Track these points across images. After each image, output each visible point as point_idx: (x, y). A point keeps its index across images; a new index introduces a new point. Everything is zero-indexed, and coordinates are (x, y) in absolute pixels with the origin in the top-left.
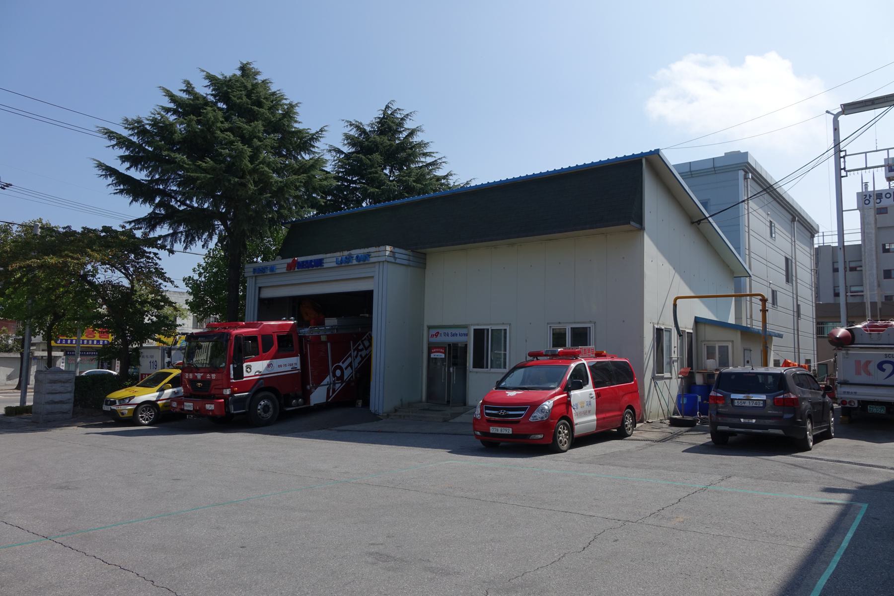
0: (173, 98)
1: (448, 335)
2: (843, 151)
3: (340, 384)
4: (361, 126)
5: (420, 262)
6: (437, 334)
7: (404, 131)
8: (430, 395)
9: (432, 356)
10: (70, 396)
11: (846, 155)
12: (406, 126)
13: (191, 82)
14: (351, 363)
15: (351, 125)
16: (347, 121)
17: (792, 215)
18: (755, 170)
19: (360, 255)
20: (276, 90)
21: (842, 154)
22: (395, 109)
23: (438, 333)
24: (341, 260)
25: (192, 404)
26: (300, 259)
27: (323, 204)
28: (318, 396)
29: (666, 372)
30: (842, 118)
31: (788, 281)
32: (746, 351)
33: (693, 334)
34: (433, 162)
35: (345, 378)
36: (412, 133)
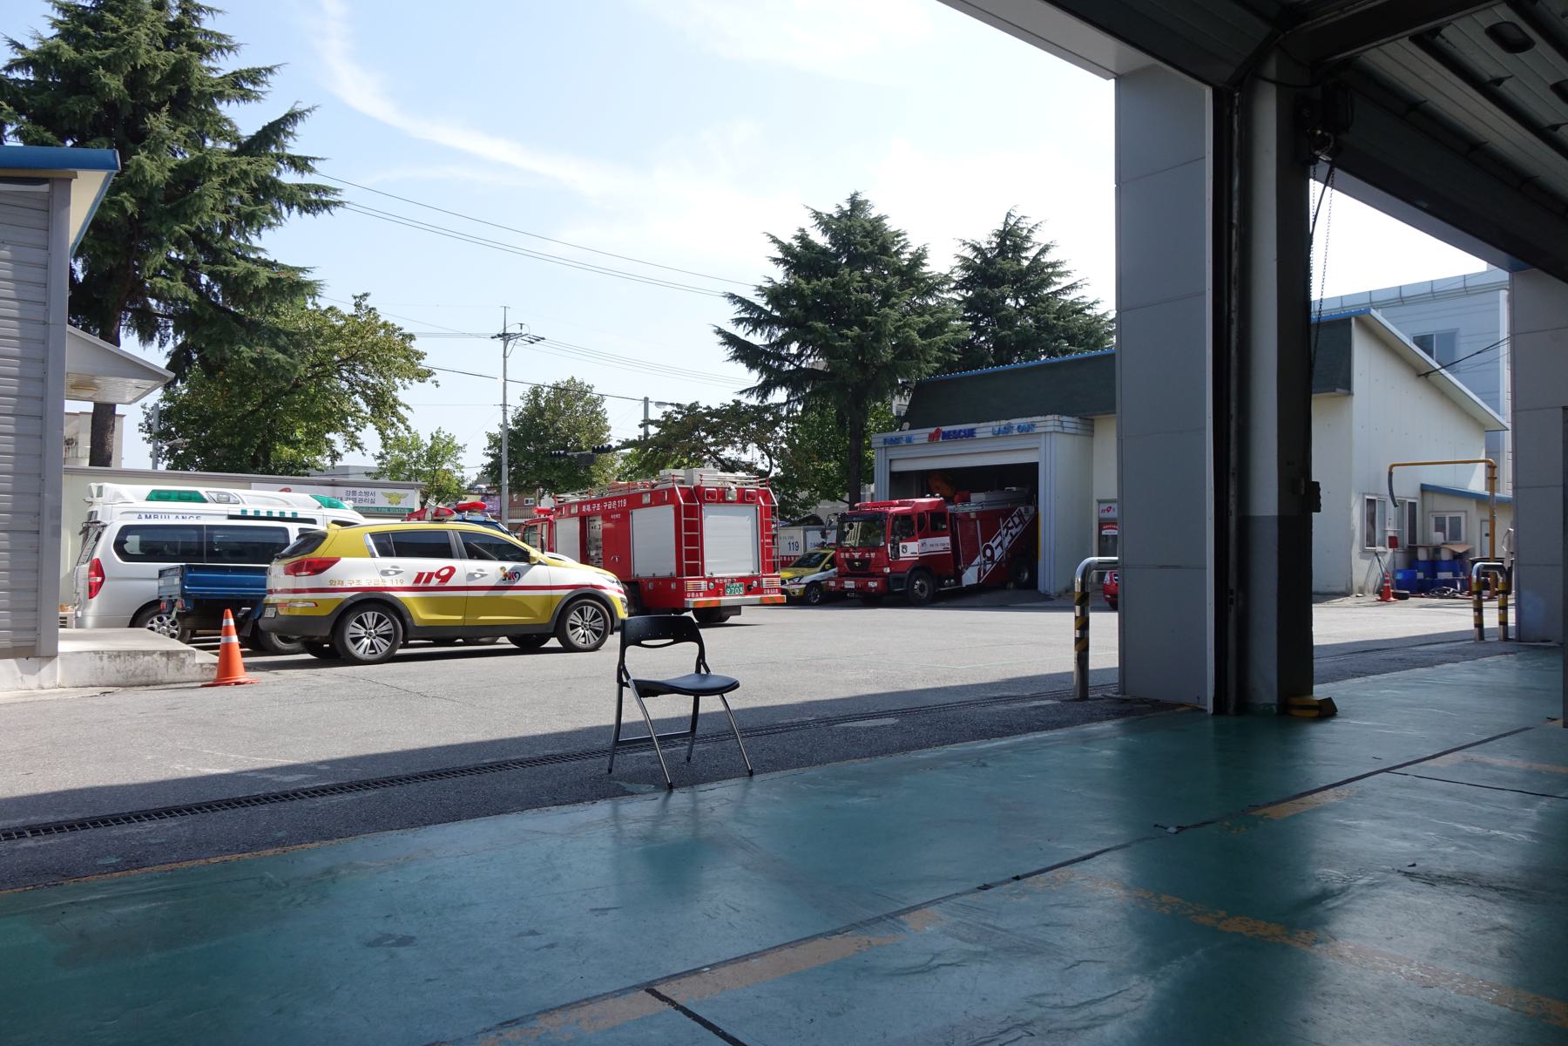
0: (785, 249)
6: (1109, 509)
7: (1032, 247)
9: (1104, 533)
14: (1001, 542)
15: (964, 244)
23: (1110, 508)
26: (945, 429)
27: (957, 360)
32: (1484, 523)
33: (1417, 505)
36: (1044, 251)
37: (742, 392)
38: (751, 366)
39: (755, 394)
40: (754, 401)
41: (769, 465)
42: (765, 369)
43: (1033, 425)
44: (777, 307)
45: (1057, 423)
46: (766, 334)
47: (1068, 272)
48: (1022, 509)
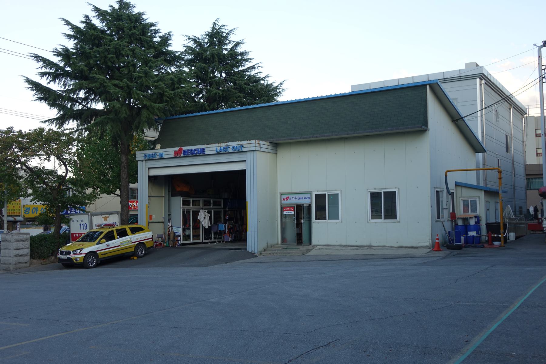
0: (75, 28)
4: (198, 40)
8: (283, 240)
9: (285, 213)
10: (27, 251)
12: (230, 39)
13: (90, 17)
15: (189, 39)
16: (187, 36)
17: (509, 104)
18: (487, 77)
19: (235, 146)
23: (288, 197)
26: (185, 148)
29: (441, 218)
31: (507, 151)
32: (487, 203)
33: (454, 193)
36: (238, 44)
37: (45, 122)
38: (52, 105)
39: (55, 123)
40: (54, 127)
41: (65, 171)
42: (61, 107)
44: (68, 64)
45: (257, 145)
46: (62, 83)
47: (249, 59)
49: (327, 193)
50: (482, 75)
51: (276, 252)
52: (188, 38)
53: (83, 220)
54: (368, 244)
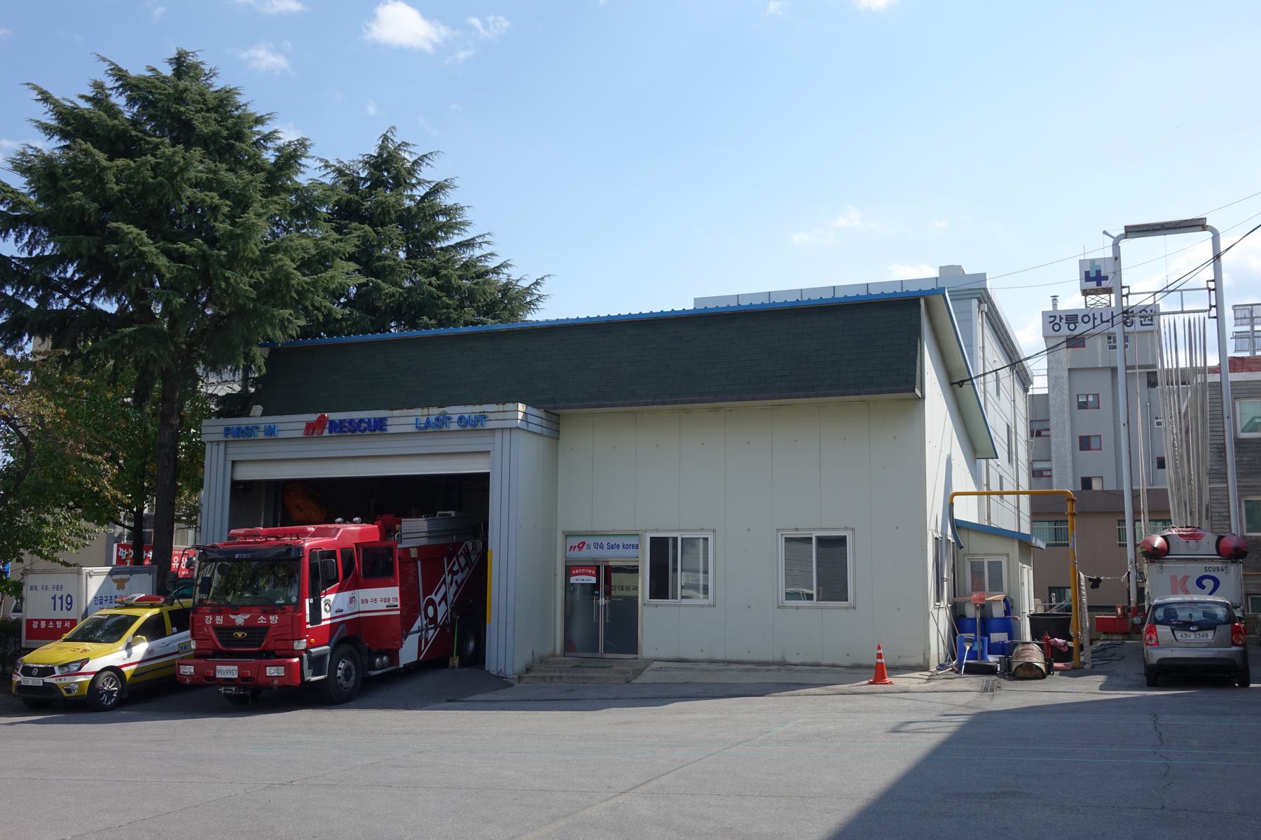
1: (602, 547)
2: (1126, 287)
3: (433, 630)
5: (554, 427)
6: (581, 546)
8: (568, 645)
9: (573, 580)
11: (1129, 293)
12: (421, 176)
15: (326, 166)
16: (321, 160)
19: (466, 416)
20: (263, 114)
21: (1125, 291)
22: (399, 143)
24: (428, 422)
25: (236, 668)
28: (409, 652)
30: (1124, 244)
34: (469, 240)
35: (439, 620)
43: (485, 417)
48: (470, 545)
49: (679, 535)
50: (983, 291)
51: (558, 674)
52: (323, 164)
53: (62, 585)
54: (778, 658)
